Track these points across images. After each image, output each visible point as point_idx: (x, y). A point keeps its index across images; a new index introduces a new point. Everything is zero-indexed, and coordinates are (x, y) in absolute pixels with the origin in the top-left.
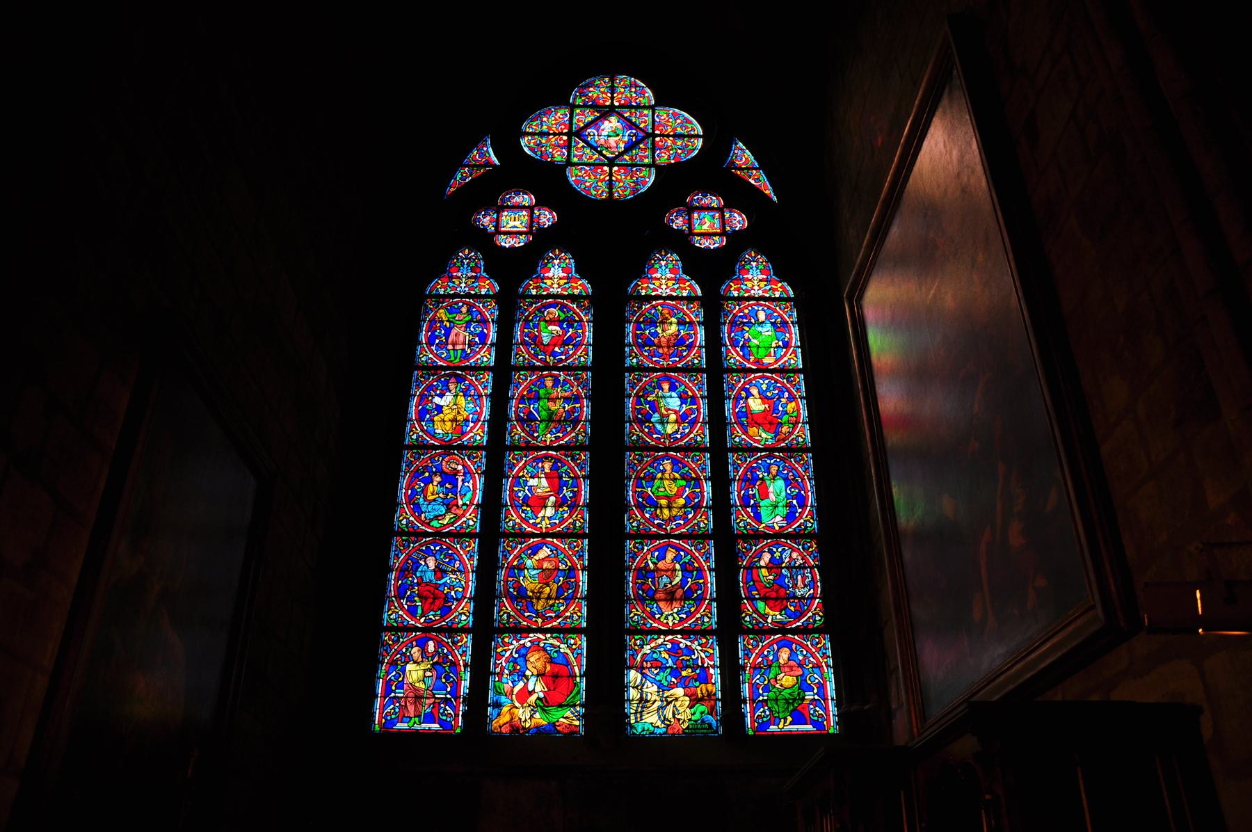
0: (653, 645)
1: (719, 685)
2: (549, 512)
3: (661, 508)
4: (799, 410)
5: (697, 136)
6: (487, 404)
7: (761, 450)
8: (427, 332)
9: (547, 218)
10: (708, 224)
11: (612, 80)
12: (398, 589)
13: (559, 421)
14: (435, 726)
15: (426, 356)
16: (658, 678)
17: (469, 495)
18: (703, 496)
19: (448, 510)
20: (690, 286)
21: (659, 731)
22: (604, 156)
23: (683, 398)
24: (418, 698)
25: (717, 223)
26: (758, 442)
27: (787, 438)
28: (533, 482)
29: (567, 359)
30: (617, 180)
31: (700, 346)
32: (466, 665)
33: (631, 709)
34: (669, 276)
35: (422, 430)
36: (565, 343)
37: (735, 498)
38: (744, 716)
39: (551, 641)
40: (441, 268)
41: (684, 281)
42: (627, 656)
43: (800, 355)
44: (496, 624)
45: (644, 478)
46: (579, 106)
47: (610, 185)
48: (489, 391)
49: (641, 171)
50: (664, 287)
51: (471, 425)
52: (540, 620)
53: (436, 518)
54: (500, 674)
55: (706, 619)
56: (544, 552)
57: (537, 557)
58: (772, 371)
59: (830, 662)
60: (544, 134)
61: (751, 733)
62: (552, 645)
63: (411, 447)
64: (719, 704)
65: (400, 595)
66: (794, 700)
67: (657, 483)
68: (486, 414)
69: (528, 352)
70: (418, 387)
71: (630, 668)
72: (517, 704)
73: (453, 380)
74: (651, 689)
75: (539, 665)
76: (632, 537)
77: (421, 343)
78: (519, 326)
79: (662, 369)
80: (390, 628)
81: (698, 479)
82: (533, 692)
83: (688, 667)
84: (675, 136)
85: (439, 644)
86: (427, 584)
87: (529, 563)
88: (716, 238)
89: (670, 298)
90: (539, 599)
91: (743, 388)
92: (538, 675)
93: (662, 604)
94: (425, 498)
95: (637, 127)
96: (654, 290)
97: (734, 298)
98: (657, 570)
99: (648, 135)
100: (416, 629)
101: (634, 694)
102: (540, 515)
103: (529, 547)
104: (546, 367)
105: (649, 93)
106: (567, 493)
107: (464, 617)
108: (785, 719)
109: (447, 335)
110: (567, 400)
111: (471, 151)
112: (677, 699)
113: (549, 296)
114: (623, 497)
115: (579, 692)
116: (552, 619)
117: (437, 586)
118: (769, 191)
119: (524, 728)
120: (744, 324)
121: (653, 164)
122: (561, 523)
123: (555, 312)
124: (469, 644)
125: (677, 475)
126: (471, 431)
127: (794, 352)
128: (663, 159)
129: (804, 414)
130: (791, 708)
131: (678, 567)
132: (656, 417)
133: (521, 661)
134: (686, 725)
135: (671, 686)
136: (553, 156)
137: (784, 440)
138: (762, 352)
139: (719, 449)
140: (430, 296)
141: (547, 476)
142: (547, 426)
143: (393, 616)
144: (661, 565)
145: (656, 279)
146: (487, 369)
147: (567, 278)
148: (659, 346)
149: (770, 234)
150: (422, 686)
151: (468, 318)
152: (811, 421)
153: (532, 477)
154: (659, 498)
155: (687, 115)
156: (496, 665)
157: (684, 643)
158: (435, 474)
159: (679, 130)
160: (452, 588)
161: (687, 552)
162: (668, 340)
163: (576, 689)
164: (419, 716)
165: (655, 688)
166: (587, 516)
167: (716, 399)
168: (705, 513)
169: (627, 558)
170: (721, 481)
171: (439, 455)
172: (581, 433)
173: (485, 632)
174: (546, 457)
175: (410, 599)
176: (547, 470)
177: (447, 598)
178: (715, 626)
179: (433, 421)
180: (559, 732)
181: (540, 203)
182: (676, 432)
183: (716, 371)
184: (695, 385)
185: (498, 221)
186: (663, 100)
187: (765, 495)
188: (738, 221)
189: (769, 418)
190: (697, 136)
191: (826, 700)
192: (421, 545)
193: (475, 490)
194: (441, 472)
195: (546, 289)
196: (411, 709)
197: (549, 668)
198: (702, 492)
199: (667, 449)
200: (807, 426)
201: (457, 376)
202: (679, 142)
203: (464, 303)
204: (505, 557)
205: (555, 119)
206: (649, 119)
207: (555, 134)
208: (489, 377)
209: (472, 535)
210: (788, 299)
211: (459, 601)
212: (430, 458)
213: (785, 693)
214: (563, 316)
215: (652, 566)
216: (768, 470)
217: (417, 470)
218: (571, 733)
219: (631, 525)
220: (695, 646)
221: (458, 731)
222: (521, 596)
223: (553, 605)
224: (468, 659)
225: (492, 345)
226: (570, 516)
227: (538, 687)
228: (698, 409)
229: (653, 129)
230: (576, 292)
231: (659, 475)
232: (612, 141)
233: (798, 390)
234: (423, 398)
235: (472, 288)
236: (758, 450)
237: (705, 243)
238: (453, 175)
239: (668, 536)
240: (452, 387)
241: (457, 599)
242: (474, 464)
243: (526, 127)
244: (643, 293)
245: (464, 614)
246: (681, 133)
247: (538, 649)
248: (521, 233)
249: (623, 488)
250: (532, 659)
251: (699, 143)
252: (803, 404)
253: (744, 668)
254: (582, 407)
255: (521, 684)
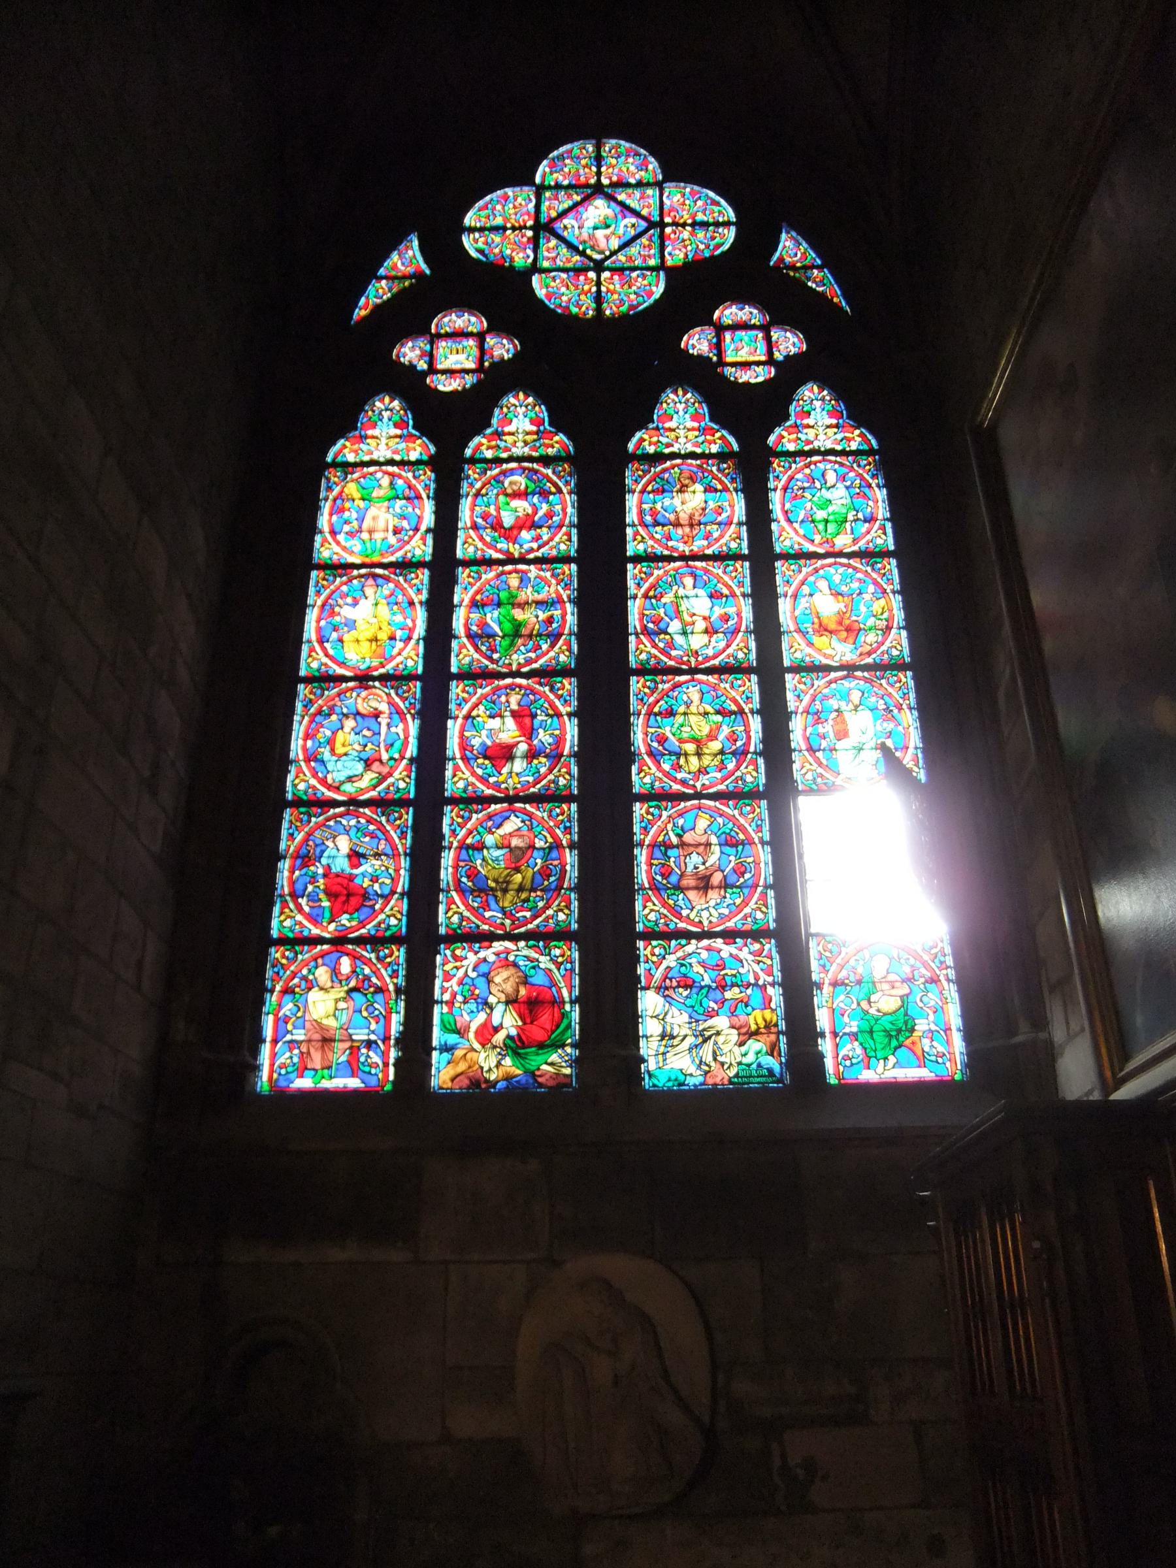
0: (680, 954)
1: (780, 1012)
2: (519, 765)
3: (686, 755)
4: (891, 610)
5: (727, 224)
6: (421, 615)
7: (836, 669)
8: (331, 515)
9: (503, 348)
10: (746, 346)
11: (598, 147)
12: (292, 883)
13: (530, 636)
14: (354, 1083)
15: (325, 550)
16: (689, 1002)
17: (398, 745)
18: (749, 738)
19: (368, 764)
20: (722, 438)
21: (691, 1081)
22: (590, 258)
23: (714, 596)
24: (327, 1041)
25: (761, 347)
26: (831, 657)
27: (874, 651)
28: (495, 723)
29: (540, 547)
30: (608, 290)
31: (740, 524)
32: (398, 990)
33: (648, 1049)
34: (691, 424)
35: (327, 655)
36: (534, 526)
37: (797, 739)
38: (821, 1056)
39: (526, 952)
40: (347, 422)
41: (713, 432)
42: (641, 970)
43: (889, 531)
44: (442, 931)
45: (660, 713)
46: (550, 188)
47: (599, 299)
48: (424, 596)
49: (644, 277)
50: (682, 440)
51: (400, 645)
52: (508, 922)
53: (350, 779)
54: (450, 1003)
55: (759, 915)
56: (513, 824)
57: (501, 832)
58: (850, 556)
59: (952, 973)
60: (495, 224)
61: (833, 1081)
62: (528, 958)
63: (309, 680)
64: (783, 1039)
65: (294, 896)
66: (899, 1031)
67: (679, 719)
68: (420, 630)
69: (481, 539)
70: (318, 593)
71: (647, 988)
72: (477, 1046)
73: (370, 581)
74: (679, 1020)
75: (509, 987)
76: (644, 798)
77: (321, 532)
78: (465, 506)
79: (683, 557)
80: (283, 941)
81: (741, 712)
82: (501, 1027)
83: (733, 985)
84: (694, 224)
85: (354, 957)
86: (337, 875)
87: (490, 840)
88: (759, 369)
89: (693, 455)
90: (505, 891)
91: (803, 583)
92: (507, 1003)
93: (692, 894)
94: (333, 751)
95: (637, 214)
96: (668, 445)
97: (787, 454)
98: (682, 845)
99: (651, 225)
100: (320, 940)
101: (649, 1027)
102: (505, 770)
103: (490, 817)
104: (510, 560)
105: (653, 164)
106: (544, 738)
107: (393, 921)
108: (886, 1059)
109: (361, 520)
110: (538, 603)
111: (387, 256)
112: (718, 1033)
113: (510, 459)
114: (628, 743)
115: (569, 1026)
116: (527, 921)
117: (351, 878)
118: (839, 300)
119: (487, 1081)
120: (804, 489)
121: (662, 266)
122: (536, 782)
123: (520, 481)
124: (402, 960)
125: (709, 709)
126: (399, 654)
127: (883, 528)
128: (676, 256)
129: (899, 616)
130: (894, 1043)
131: (714, 840)
132: (675, 626)
133: (481, 983)
134: (732, 1072)
135: (710, 1014)
136: (512, 259)
137: (869, 654)
138: (832, 528)
139: (770, 670)
140: (335, 465)
141: (514, 714)
142: (512, 644)
143: (288, 923)
144: (688, 837)
145: (671, 430)
146: (421, 564)
147: (537, 433)
148: (677, 524)
149: (838, 358)
150: (331, 1023)
151: (392, 493)
152: (910, 625)
153: (492, 717)
154: (681, 741)
155: (712, 194)
156: (444, 990)
157: (727, 950)
158: (346, 716)
159: (700, 217)
160: (375, 879)
161: (732, 818)
162: (691, 517)
163: (565, 1022)
164: (329, 1068)
165: (685, 1017)
166: (575, 770)
167: (764, 595)
168: (754, 762)
169: (636, 828)
170: (774, 713)
171: (352, 689)
172: (563, 654)
173: (423, 941)
174: (511, 687)
175: (314, 899)
176: (514, 706)
177: (365, 895)
178: (772, 925)
179: (341, 640)
180: (541, 1085)
181: (494, 328)
182: (707, 646)
183: (762, 557)
184: (732, 579)
185: (431, 357)
186: (673, 172)
187: (842, 734)
188: (789, 343)
189: (847, 622)
190: (727, 224)
191: (947, 1030)
192: (328, 819)
193: (406, 738)
194: (358, 713)
195: (507, 449)
196: (317, 1059)
197: (523, 992)
198: (747, 732)
199: (693, 671)
200: (904, 633)
201: (375, 576)
202: (701, 234)
203: (386, 473)
204: (453, 832)
205: (510, 205)
206: (654, 202)
207: (514, 229)
208: (425, 575)
209: (404, 803)
210: (870, 452)
211: (387, 898)
212: (339, 695)
213: (885, 1023)
214: (532, 486)
215: (675, 840)
216: (847, 696)
217: (319, 712)
218: (560, 1085)
219: (640, 781)
220: (744, 954)
221: (388, 1087)
222: (480, 890)
223: (527, 900)
224: (401, 981)
225: (428, 530)
226: (550, 770)
227: (509, 1022)
228: (739, 615)
229: (661, 215)
230: (550, 451)
231: (682, 709)
232: (600, 234)
233: (890, 582)
234: (328, 609)
235: (396, 452)
236: (827, 669)
237: (744, 377)
238: (362, 291)
239: (698, 796)
240: (369, 591)
241: (382, 896)
242: (404, 700)
243: (470, 219)
244: (651, 450)
245: (393, 916)
246: (703, 221)
247: (507, 964)
248: (467, 371)
249: (627, 727)
250: (497, 980)
251: (730, 234)
252: (896, 602)
253: (819, 986)
254: (564, 616)
255: (482, 1017)
